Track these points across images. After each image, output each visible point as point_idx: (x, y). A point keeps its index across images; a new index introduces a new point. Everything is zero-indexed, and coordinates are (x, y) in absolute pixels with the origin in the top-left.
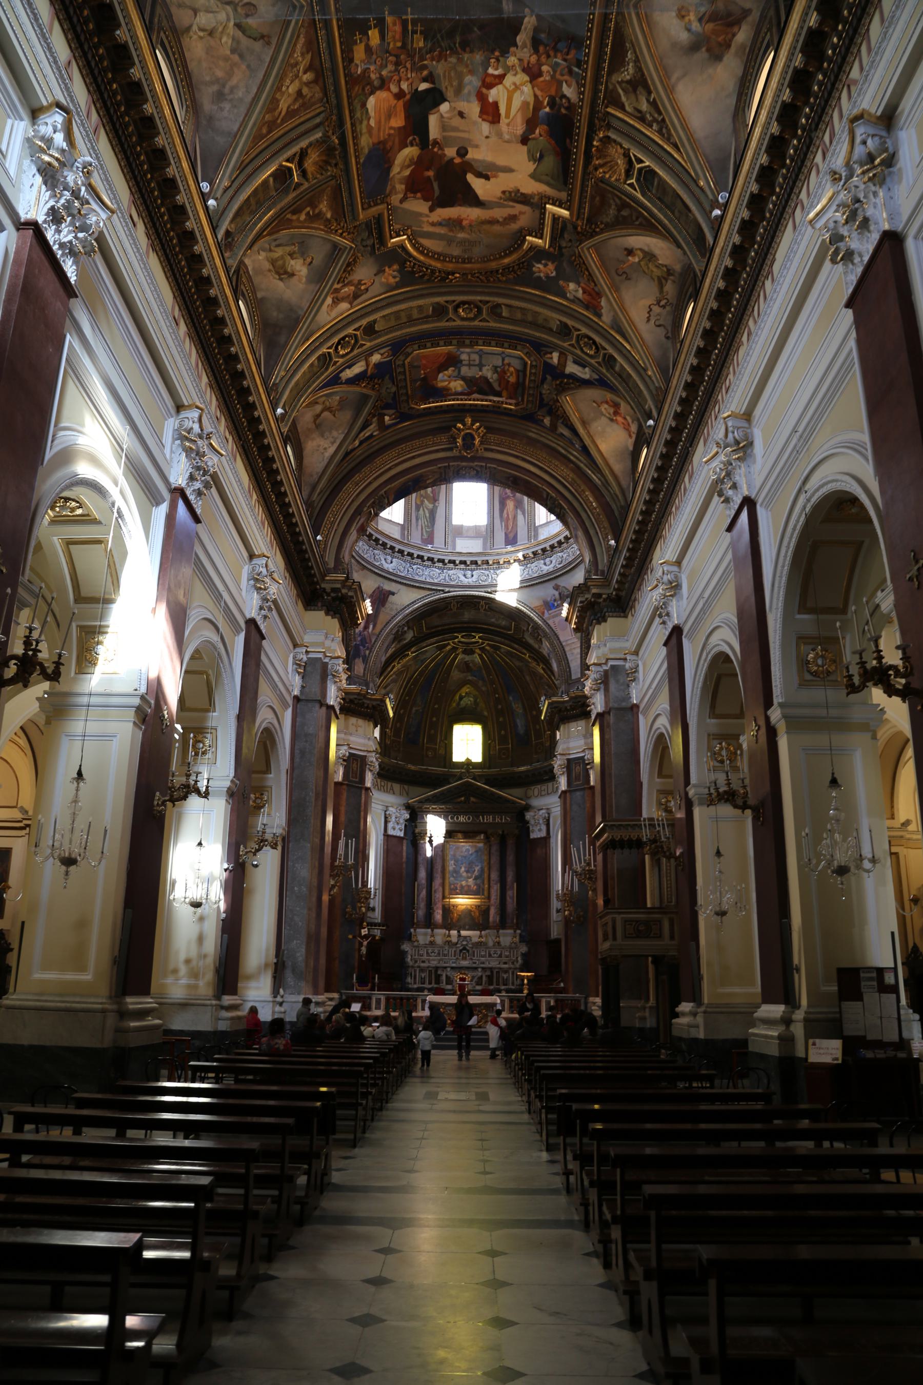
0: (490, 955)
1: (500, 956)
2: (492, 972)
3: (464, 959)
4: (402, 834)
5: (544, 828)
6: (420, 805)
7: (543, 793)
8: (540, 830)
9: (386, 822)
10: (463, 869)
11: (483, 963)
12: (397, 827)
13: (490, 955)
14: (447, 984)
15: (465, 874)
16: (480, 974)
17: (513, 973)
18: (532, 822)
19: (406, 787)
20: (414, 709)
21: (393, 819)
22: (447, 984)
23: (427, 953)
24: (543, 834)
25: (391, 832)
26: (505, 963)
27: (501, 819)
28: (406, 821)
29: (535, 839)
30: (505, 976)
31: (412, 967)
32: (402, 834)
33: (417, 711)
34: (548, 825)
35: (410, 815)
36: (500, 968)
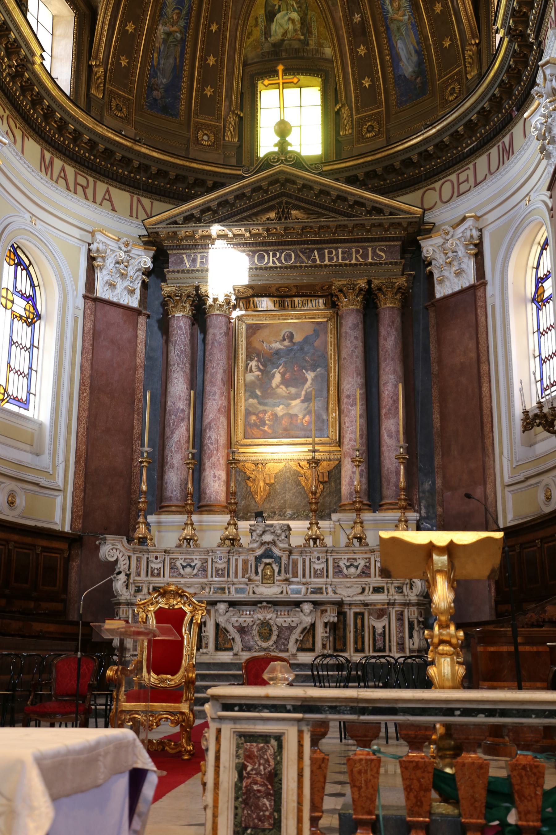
0: (338, 571)
1: (365, 573)
2: (342, 614)
3: (267, 580)
4: (134, 302)
5: (470, 266)
6: (173, 228)
7: (463, 188)
8: (459, 273)
9: (91, 270)
10: (277, 378)
11: (318, 591)
12: (121, 285)
13: (338, 571)
14: (218, 648)
15: (282, 390)
16: (308, 620)
17: (400, 617)
18: (440, 259)
19: (146, 202)
20: (161, 29)
21: (110, 263)
22: (218, 648)
23: (173, 567)
24: (469, 279)
25: (101, 291)
26: (378, 590)
27: (364, 256)
28: (147, 273)
29: (446, 298)
30: (379, 625)
31: (129, 604)
32: (134, 302)
33: (168, 34)
34: (479, 256)
35: (155, 259)
36: (366, 605)
